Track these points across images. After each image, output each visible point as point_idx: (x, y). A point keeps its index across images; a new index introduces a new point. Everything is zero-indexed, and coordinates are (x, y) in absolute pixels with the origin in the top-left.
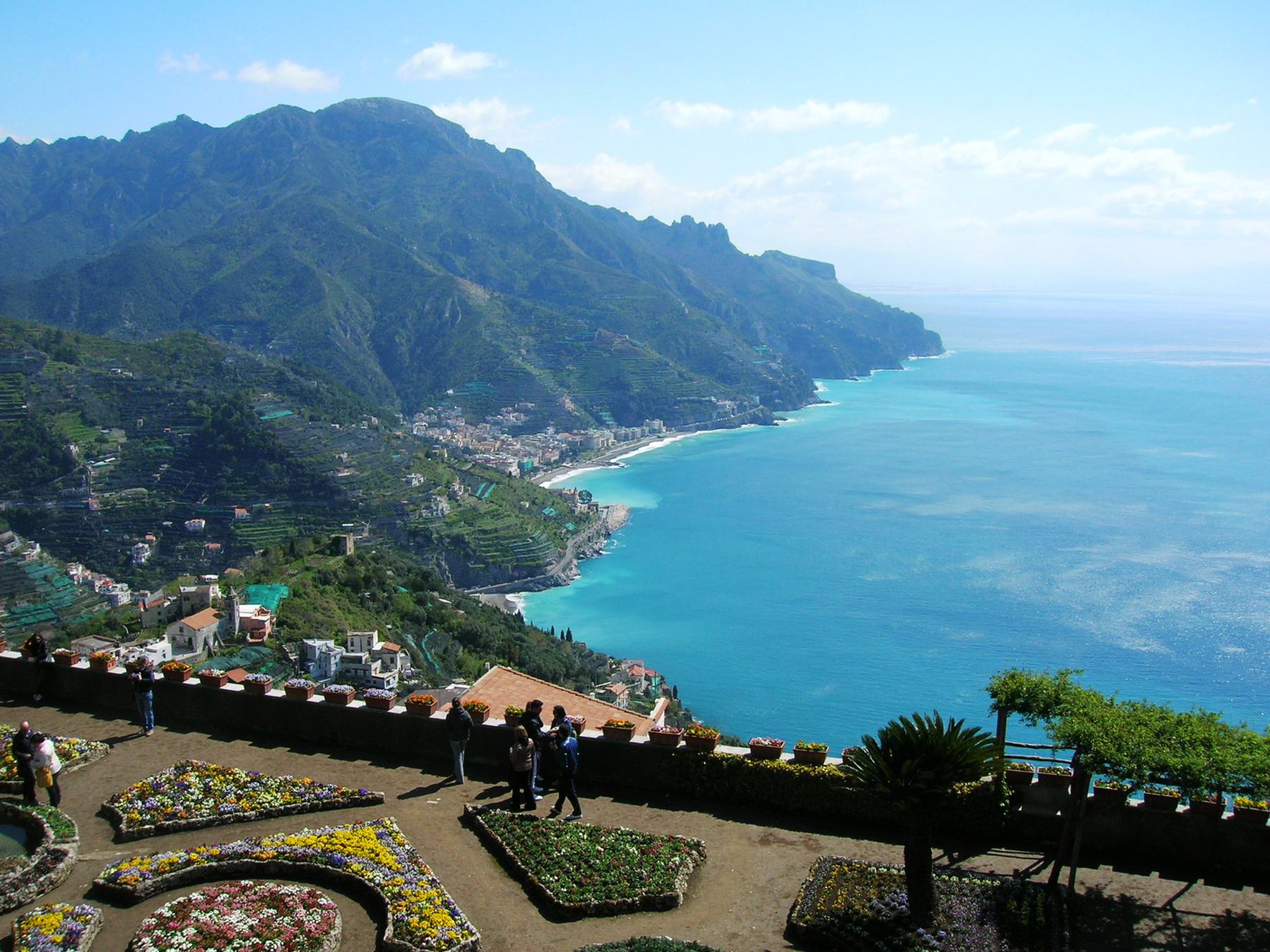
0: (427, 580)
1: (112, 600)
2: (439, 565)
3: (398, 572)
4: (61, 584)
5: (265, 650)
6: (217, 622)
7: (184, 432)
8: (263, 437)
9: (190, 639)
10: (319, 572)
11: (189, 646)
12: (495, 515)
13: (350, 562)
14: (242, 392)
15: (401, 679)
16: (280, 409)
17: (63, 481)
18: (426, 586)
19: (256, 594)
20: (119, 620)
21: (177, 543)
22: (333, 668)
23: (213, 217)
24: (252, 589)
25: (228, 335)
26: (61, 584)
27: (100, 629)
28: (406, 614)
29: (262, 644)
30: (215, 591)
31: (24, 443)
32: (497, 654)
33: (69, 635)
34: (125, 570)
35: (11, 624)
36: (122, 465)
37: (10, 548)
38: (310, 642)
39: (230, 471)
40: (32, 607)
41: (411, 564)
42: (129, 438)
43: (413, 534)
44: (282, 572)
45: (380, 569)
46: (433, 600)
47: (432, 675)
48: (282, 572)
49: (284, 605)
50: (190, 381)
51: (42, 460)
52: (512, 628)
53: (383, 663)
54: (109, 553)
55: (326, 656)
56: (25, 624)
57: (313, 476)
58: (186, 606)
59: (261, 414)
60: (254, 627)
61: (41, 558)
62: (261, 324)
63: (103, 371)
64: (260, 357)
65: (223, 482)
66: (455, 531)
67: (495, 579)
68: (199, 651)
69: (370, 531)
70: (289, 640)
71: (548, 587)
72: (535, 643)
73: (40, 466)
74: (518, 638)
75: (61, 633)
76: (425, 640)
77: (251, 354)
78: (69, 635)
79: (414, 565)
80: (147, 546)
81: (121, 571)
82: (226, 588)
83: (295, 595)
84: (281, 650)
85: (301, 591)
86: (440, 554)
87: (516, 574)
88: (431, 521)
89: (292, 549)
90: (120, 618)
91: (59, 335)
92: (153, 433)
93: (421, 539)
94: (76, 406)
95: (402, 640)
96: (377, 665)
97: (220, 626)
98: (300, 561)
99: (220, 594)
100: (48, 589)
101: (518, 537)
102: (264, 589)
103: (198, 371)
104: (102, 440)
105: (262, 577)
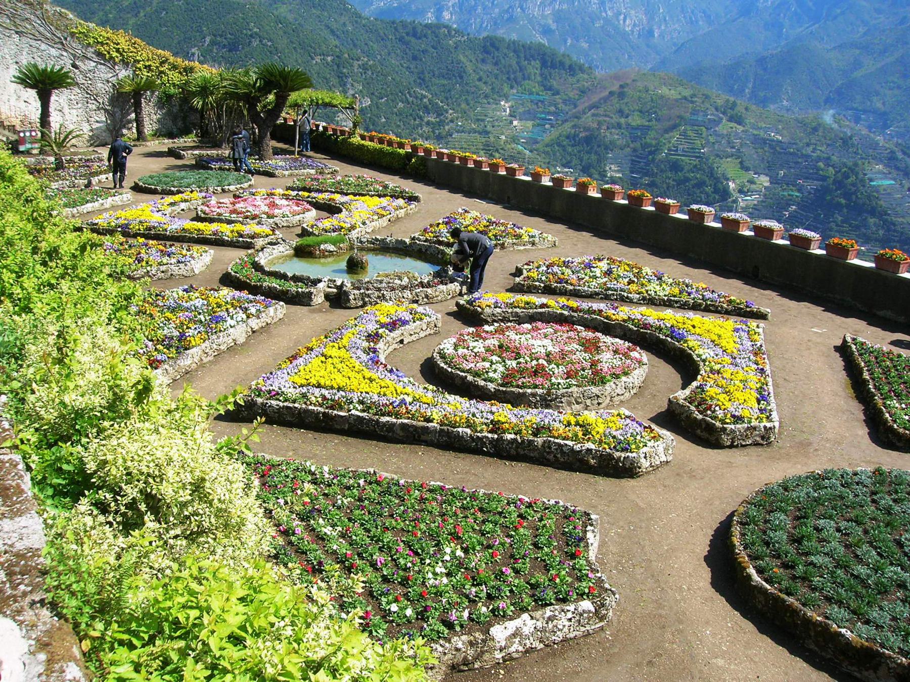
7: (811, 186)
8: (869, 197)
14: (860, 162)
16: (886, 178)
17: (720, 206)
23: (860, 29)
25: (857, 120)
31: (698, 176)
36: (763, 201)
39: (840, 218)
42: (771, 183)
50: (823, 149)
51: (708, 189)
57: (902, 233)
59: (871, 180)
62: (884, 114)
63: (762, 133)
64: (879, 139)
65: (833, 225)
73: (707, 193)
77: (872, 135)
91: (734, 104)
92: (789, 182)
94: (738, 155)
103: (829, 142)
104: (752, 182)
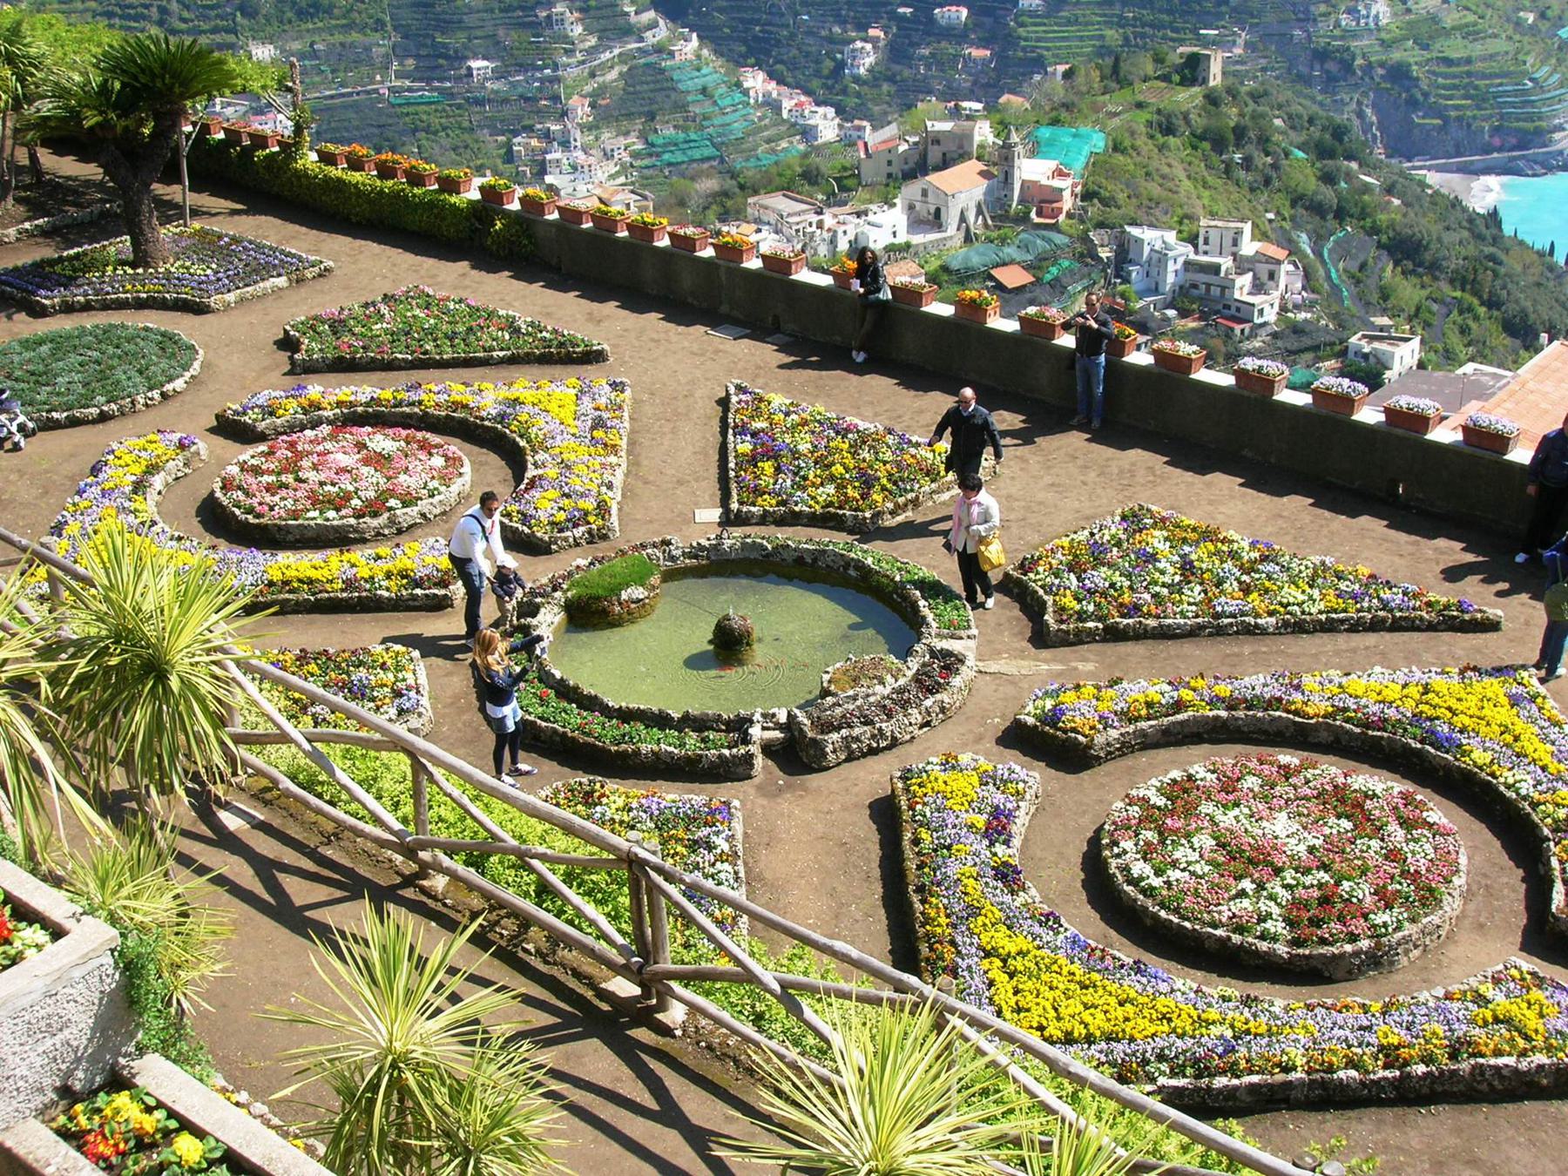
0: (1341, 141)
1: (808, 133)
2: (1360, 115)
3: (1293, 121)
4: (728, 101)
5: (1059, 239)
6: (984, 184)
9: (938, 211)
10: (1159, 112)
11: (936, 220)
12: (1470, 33)
13: (1212, 99)
15: (1283, 309)
18: (1340, 150)
19: (1051, 142)
20: (823, 169)
21: (918, 45)
22: (1171, 278)
24: (1045, 132)
26: (728, 101)
27: (792, 180)
28: (1301, 197)
29: (1054, 227)
30: (983, 133)
32: (1452, 281)
33: (742, 187)
34: (831, 85)
35: (646, 162)
37: (651, 38)
38: (1134, 231)
40: (682, 136)
41: (1315, 108)
43: (1322, 55)
44: (1096, 108)
45: (1263, 116)
46: (1349, 176)
47: (1335, 308)
48: (1096, 108)
49: (1097, 165)
52: (1479, 237)
53: (1255, 278)
54: (808, 54)
55: (1160, 258)
56: (670, 164)
58: (934, 154)
60: (1045, 199)
61: (699, 57)
66: (1396, 56)
67: (1457, 146)
68: (951, 230)
69: (1247, 45)
70: (1101, 225)
71: (1550, 169)
72: (1518, 268)
74: (1492, 258)
75: (730, 184)
76: (1330, 245)
78: (742, 187)
79: (1321, 113)
80: (869, 47)
81: (825, 86)
82: (1002, 127)
83: (1116, 149)
84: (1085, 239)
85: (1127, 143)
86: (1365, 94)
87: (1497, 141)
88: (1354, 35)
89: (1115, 69)
90: (828, 167)
93: (1333, 67)
95: (1290, 241)
96: (1245, 280)
97: (988, 193)
98: (1127, 92)
99: (991, 139)
100: (708, 108)
101: (1506, 75)
102: (1064, 135)
105: (1061, 114)
